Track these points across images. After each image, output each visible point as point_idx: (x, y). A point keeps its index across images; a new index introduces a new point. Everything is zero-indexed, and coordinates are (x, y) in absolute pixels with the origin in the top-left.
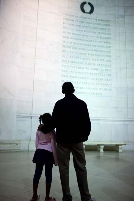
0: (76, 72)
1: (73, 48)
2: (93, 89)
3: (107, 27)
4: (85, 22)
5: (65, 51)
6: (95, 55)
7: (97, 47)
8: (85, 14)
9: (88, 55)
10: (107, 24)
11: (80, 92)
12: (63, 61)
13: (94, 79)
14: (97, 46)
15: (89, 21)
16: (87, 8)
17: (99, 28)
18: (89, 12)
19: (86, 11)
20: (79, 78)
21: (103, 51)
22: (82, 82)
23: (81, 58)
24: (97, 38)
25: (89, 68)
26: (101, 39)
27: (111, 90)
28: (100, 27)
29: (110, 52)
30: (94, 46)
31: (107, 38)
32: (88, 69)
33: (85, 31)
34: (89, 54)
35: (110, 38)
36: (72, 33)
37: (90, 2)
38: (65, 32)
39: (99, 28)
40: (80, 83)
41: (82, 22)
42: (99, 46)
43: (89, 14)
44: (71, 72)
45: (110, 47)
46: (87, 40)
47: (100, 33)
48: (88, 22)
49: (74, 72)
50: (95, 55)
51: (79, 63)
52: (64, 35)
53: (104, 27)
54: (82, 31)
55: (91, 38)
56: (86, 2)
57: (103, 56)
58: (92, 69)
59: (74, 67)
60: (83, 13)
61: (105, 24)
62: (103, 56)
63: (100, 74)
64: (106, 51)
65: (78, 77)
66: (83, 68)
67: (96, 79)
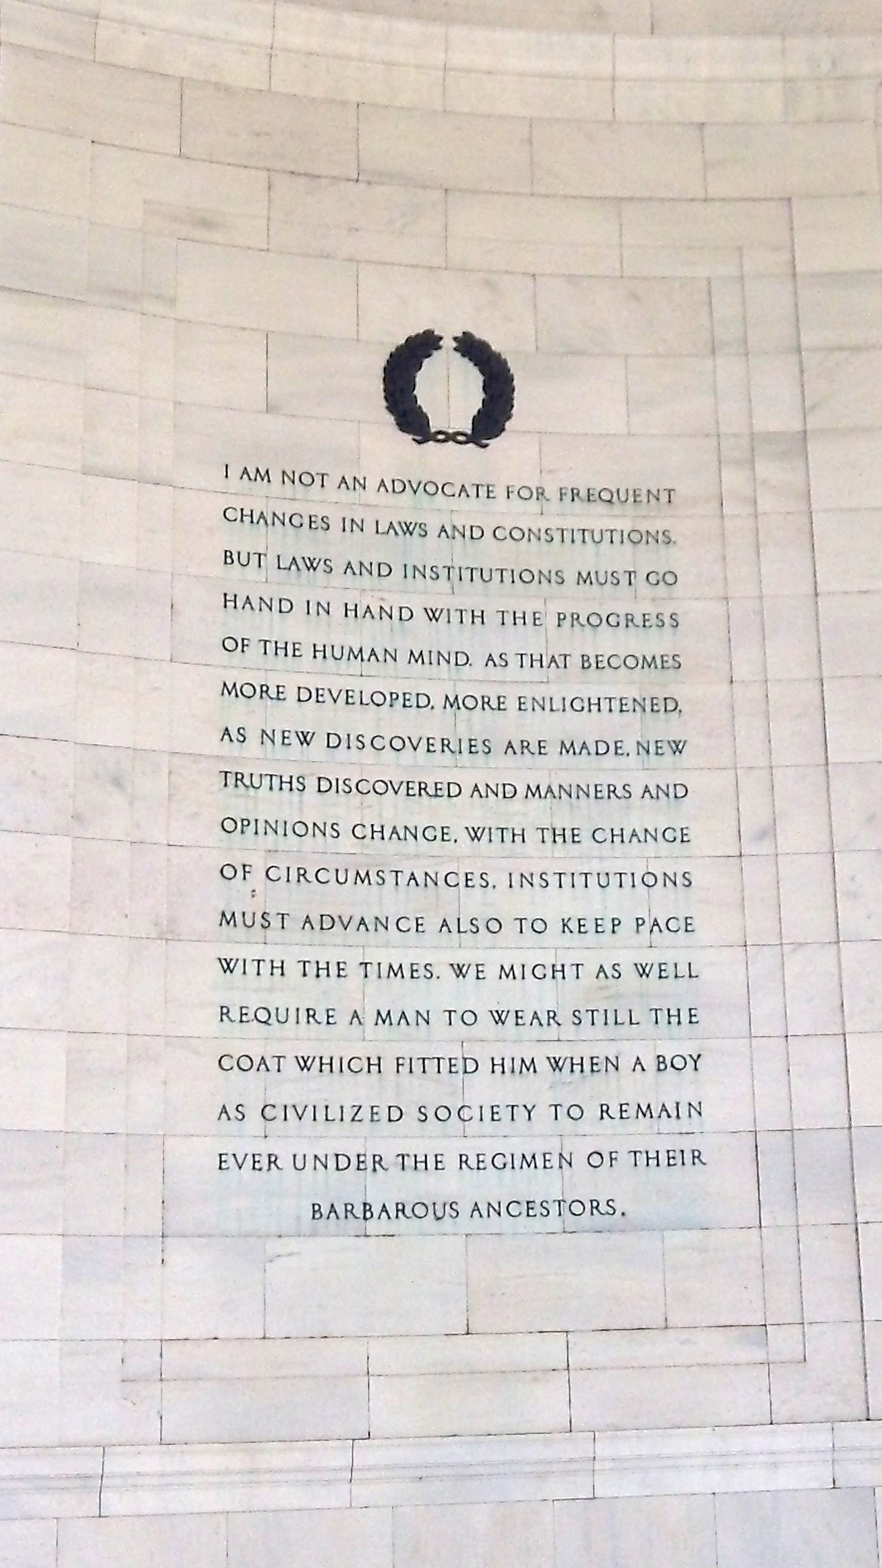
2: (529, 1161)
3: (647, 559)
6: (533, 837)
9: (464, 837)
10: (643, 526)
12: (227, 919)
13: (529, 1066)
14: (553, 749)
15: (468, 512)
17: (570, 577)
18: (462, 421)
20: (389, 1065)
21: (612, 791)
23: (403, 879)
27: (697, 1156)
29: (677, 793)
30: (525, 746)
31: (648, 663)
33: (433, 615)
35: (669, 663)
37: (480, 334)
39: (570, 577)
40: (396, 1114)
42: (567, 748)
43: (471, 445)
44: (311, 1014)
45: (677, 748)
46: (452, 703)
49: (341, 1018)
50: (533, 837)
51: (381, 923)
53: (618, 558)
54: (405, 615)
57: (617, 836)
58: (507, 972)
61: (625, 525)
62: (617, 836)
63: (586, 1018)
64: (637, 790)
65: (374, 1065)
67: (556, 1065)
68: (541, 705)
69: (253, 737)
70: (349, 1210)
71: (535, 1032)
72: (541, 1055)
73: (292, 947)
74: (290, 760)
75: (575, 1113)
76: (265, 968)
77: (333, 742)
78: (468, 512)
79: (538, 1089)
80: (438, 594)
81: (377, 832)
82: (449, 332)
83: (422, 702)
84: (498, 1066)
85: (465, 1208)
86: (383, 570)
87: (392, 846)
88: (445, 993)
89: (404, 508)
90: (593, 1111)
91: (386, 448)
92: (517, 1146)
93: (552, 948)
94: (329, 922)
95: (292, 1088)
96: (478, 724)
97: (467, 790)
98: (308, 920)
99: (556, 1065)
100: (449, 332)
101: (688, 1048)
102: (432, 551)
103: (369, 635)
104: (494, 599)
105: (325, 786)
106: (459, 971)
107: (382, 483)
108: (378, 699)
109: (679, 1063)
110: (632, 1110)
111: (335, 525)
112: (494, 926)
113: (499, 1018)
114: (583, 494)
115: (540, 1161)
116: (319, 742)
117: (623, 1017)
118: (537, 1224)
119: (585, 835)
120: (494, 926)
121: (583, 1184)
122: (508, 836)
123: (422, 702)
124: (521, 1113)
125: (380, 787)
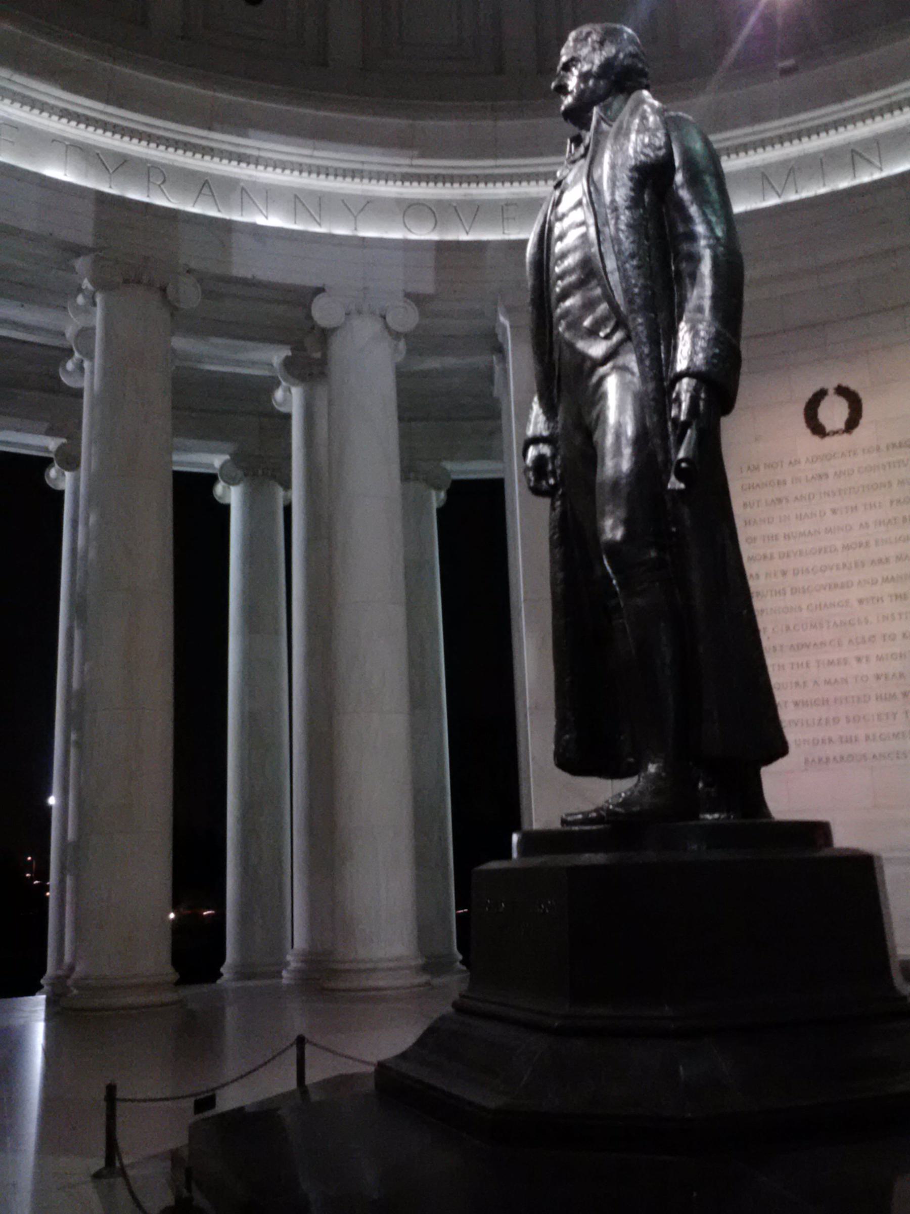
0: (816, 682)
2: (896, 736)
4: (831, 472)
8: (827, 440)
9: (856, 604)
11: (842, 758)
13: (893, 696)
16: (834, 413)
18: (841, 425)
19: (828, 428)
22: (847, 718)
23: (832, 624)
37: (845, 383)
40: (836, 720)
43: (845, 436)
44: (797, 684)
46: (846, 547)
56: (826, 387)
59: (808, 665)
60: (816, 439)
65: (825, 702)
70: (820, 760)
77: (796, 573)
81: (819, 607)
82: (831, 386)
86: (811, 497)
89: (818, 467)
100: (831, 386)
105: (794, 590)
106: (859, 660)
107: (807, 459)
113: (878, 677)
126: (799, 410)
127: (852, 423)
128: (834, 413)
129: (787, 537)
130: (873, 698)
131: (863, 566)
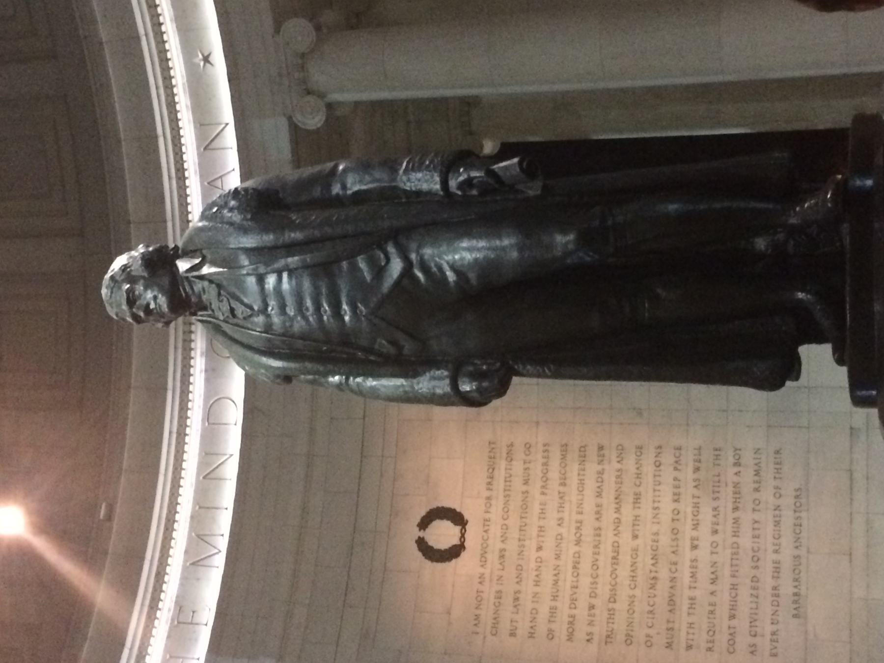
1: (615, 602)
2: (777, 523)
5: (628, 635)
6: (637, 512)
7: (604, 501)
8: (466, 544)
10: (504, 455)
11: (796, 580)
12: (669, 646)
13: (736, 521)
15: (495, 530)
16: (443, 534)
17: (524, 488)
19: (456, 541)
23: (653, 569)
24: (566, 498)
25: (693, 539)
26: (568, 482)
27: (777, 452)
28: (517, 484)
30: (598, 513)
31: (564, 457)
32: (696, 542)
33: (540, 548)
34: (635, 537)
36: (553, 604)
37: (418, 520)
38: (550, 631)
39: (524, 488)
40: (755, 579)
41: (502, 557)
42: (599, 495)
43: (467, 527)
44: (711, 612)
46: (578, 542)
47: (543, 487)
48: (499, 534)
49: (713, 599)
52: (564, 637)
53: (518, 467)
54: (540, 560)
55: (565, 524)
57: (638, 476)
58: (696, 526)
60: (464, 555)
62: (638, 476)
64: (619, 466)
65: (734, 587)
66: (692, 561)
67: (736, 509)
68: (580, 505)
69: (590, 629)
70: (795, 602)
71: (721, 516)
72: (731, 516)
73: (682, 620)
74: (601, 614)
75: (757, 502)
76: (691, 631)
78: (495, 530)
79: (746, 517)
80: (531, 545)
82: (417, 533)
83: (578, 555)
84: (736, 534)
85: (796, 552)
86: (519, 568)
87: (639, 572)
88: (704, 554)
89: (493, 557)
90: (757, 495)
91: (465, 563)
92: (770, 528)
93: (687, 507)
94: (671, 601)
95: (742, 624)
96: (587, 531)
97: (616, 539)
98: (670, 611)
99: (736, 509)
100: (417, 533)
101: (731, 453)
102: (512, 546)
103: (548, 577)
104: (534, 520)
105: (613, 599)
106: (694, 547)
107: (482, 566)
108: (575, 574)
109: (737, 457)
110: (756, 478)
111: (500, 588)
112: (675, 531)
114: (489, 480)
115: (778, 519)
116: (594, 601)
117: (716, 479)
118: (805, 522)
119: (637, 490)
120: (675, 531)
121: (788, 501)
122: (637, 523)
123: (578, 555)
124: (756, 526)
125: (614, 576)
126: (429, 566)
127: (458, 518)
128: (443, 534)
129: (555, 598)
130: (735, 539)
131: (600, 529)
